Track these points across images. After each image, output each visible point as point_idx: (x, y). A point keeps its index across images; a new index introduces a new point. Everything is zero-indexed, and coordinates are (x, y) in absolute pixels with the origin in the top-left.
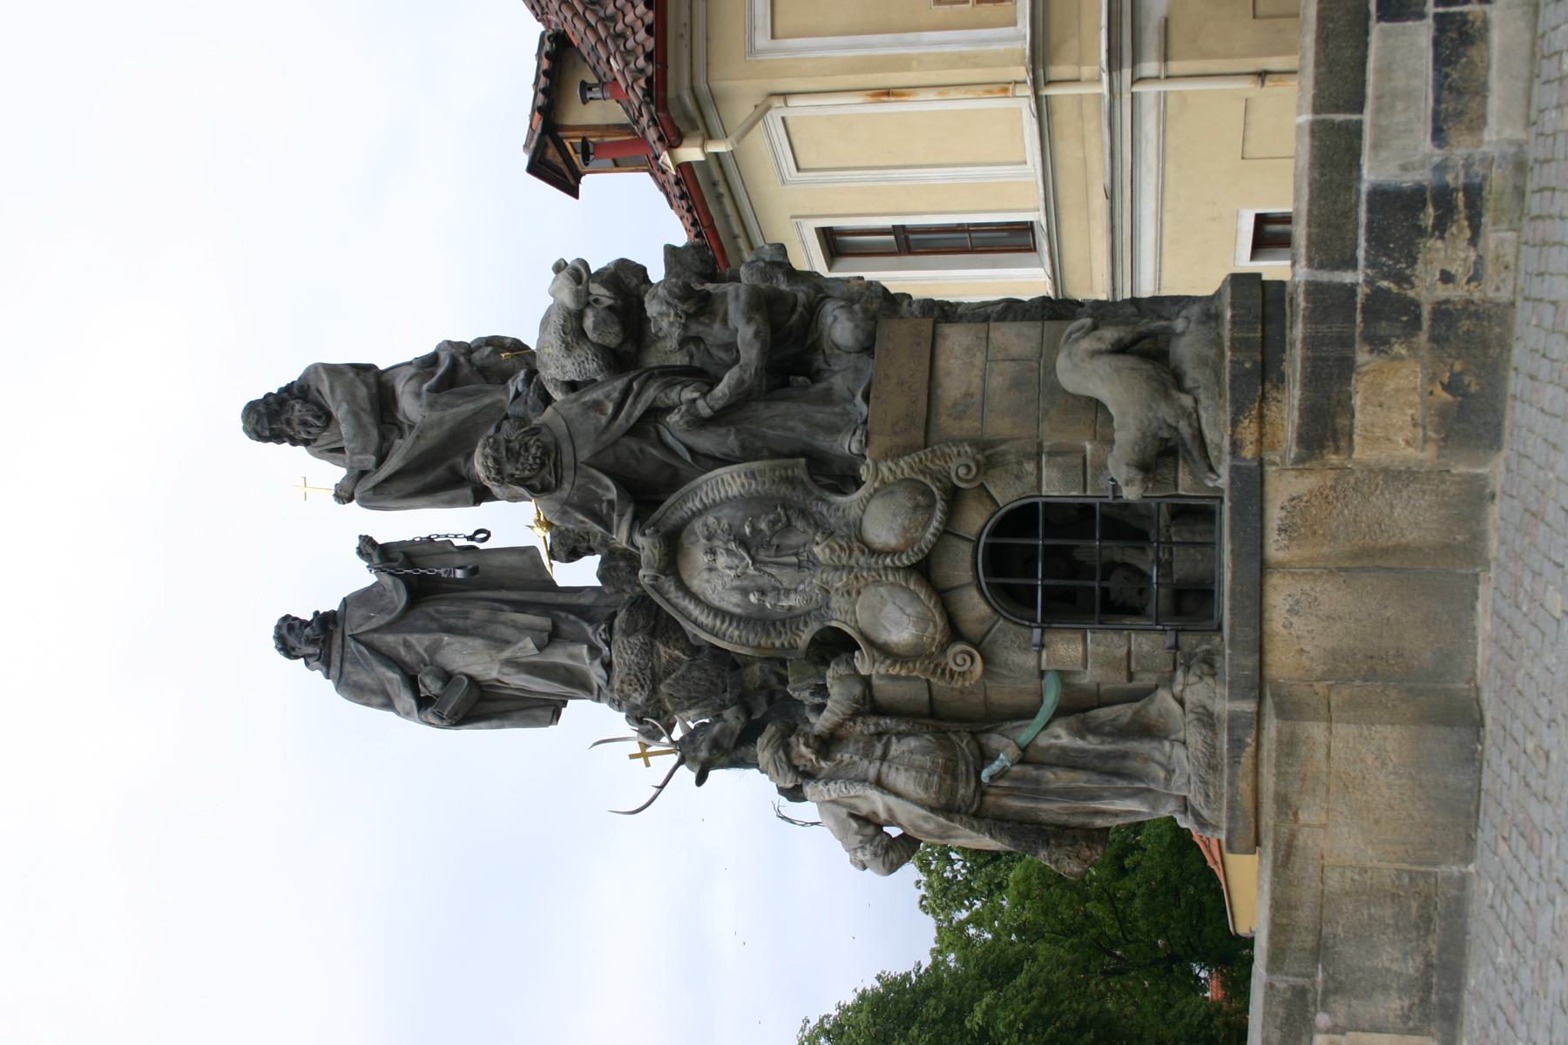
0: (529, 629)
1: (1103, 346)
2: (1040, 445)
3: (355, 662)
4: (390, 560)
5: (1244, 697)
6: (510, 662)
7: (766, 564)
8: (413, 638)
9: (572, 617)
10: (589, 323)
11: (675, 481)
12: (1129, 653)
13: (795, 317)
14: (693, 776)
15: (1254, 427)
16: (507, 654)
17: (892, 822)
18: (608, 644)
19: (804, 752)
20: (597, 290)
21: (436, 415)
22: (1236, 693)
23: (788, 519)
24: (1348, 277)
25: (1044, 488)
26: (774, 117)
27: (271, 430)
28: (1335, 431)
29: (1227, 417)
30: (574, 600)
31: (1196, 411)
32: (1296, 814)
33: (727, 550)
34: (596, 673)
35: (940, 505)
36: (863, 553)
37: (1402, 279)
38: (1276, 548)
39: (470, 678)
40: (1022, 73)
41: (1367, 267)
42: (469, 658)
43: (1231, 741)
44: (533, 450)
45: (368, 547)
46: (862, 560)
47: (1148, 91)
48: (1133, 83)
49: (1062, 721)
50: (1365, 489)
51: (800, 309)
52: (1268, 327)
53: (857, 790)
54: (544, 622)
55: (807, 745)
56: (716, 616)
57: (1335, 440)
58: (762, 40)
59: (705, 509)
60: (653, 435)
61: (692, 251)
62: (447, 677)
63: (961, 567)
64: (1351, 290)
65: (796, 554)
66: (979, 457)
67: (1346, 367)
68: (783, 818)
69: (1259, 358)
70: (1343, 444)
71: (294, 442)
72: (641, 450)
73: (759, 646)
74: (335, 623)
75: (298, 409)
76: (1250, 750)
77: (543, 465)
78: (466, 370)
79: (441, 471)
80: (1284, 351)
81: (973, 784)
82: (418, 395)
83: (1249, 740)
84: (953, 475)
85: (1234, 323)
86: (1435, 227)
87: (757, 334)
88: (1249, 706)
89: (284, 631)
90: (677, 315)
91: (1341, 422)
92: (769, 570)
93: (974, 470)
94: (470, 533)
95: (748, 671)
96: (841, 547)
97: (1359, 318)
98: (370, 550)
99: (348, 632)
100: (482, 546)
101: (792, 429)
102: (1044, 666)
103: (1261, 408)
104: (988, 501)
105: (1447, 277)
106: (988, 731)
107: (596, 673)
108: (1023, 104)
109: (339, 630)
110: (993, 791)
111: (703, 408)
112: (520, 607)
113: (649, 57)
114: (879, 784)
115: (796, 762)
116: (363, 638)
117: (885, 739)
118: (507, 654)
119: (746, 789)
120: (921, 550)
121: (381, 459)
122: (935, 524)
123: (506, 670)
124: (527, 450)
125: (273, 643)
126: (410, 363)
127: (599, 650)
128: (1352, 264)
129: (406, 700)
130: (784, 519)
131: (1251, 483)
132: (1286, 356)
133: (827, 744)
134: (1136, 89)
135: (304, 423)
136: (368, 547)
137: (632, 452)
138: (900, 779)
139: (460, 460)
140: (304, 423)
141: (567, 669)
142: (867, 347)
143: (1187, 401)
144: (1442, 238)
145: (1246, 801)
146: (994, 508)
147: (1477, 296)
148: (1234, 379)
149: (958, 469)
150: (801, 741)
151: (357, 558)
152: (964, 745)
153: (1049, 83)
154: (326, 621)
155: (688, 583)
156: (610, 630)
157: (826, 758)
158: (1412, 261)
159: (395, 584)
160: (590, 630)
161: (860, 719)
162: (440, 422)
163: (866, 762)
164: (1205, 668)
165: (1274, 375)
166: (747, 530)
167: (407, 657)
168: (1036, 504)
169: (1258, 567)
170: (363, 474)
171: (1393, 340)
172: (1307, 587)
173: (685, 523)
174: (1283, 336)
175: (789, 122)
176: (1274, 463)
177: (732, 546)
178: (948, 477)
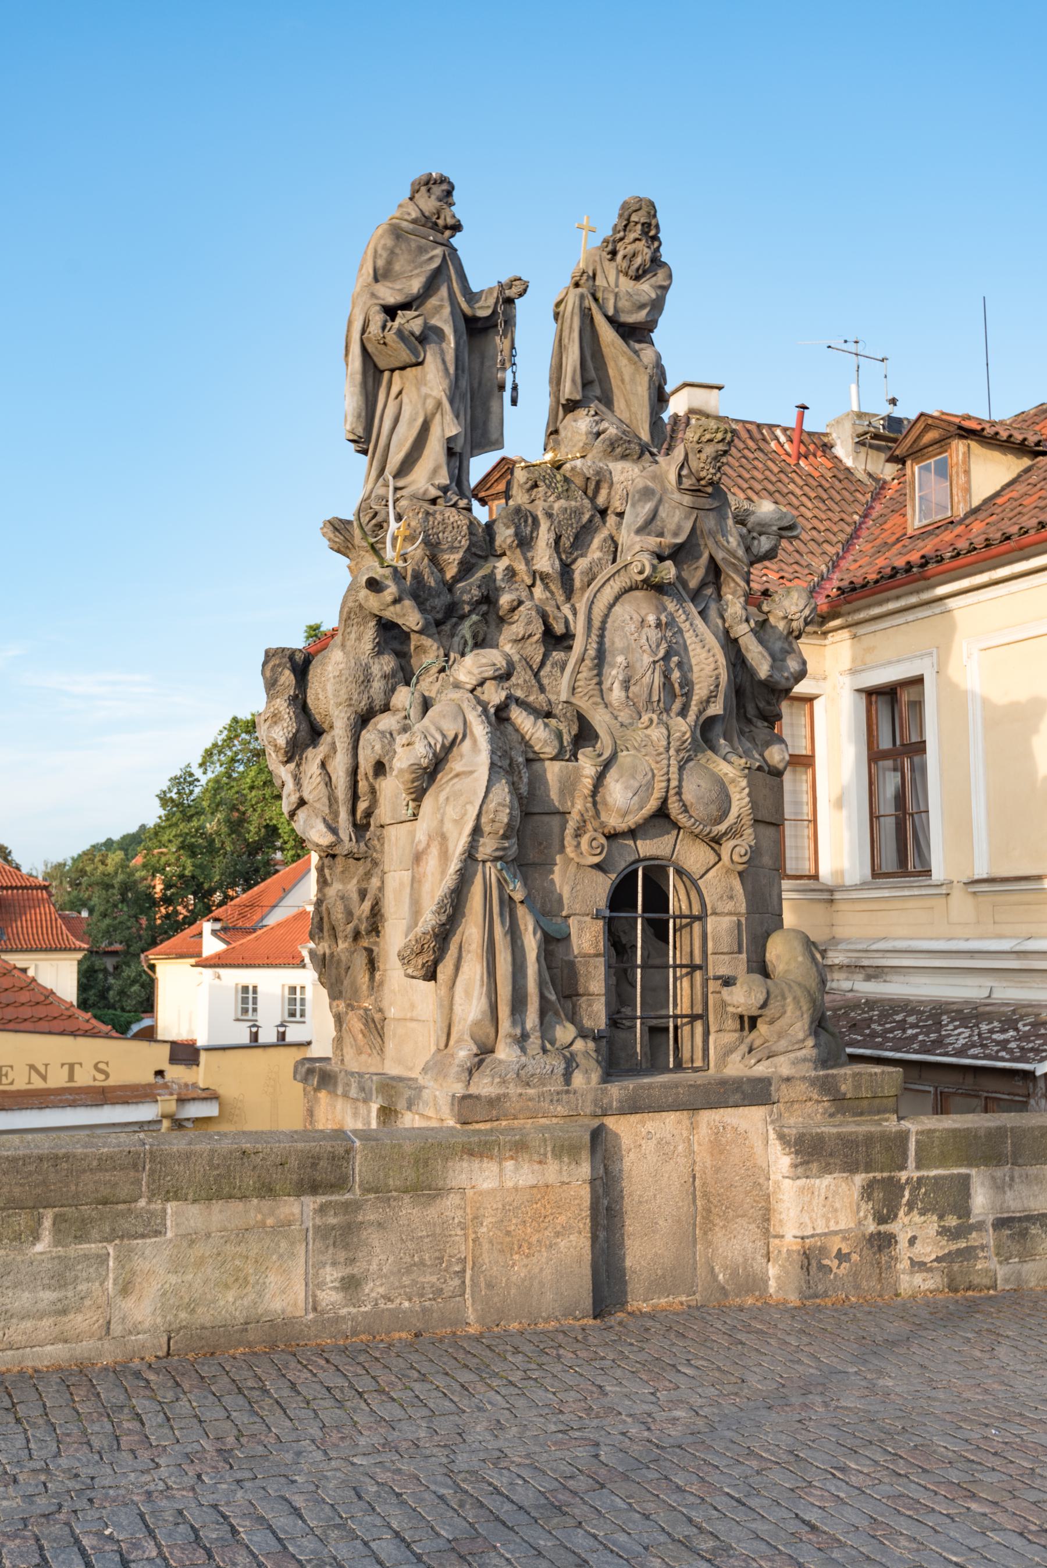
24: (911, 1162)
28: (807, 1163)
32: (512, 1158)
37: (911, 1206)
50: (754, 1193)
57: (802, 1164)
67: (851, 1168)
69: (848, 1096)
70: (800, 1170)
86: (943, 1227)
105: (912, 1241)
121: (611, 320)
128: (918, 1168)
144: (939, 1233)
147: (900, 1266)
158: (922, 1213)
171: (870, 1204)
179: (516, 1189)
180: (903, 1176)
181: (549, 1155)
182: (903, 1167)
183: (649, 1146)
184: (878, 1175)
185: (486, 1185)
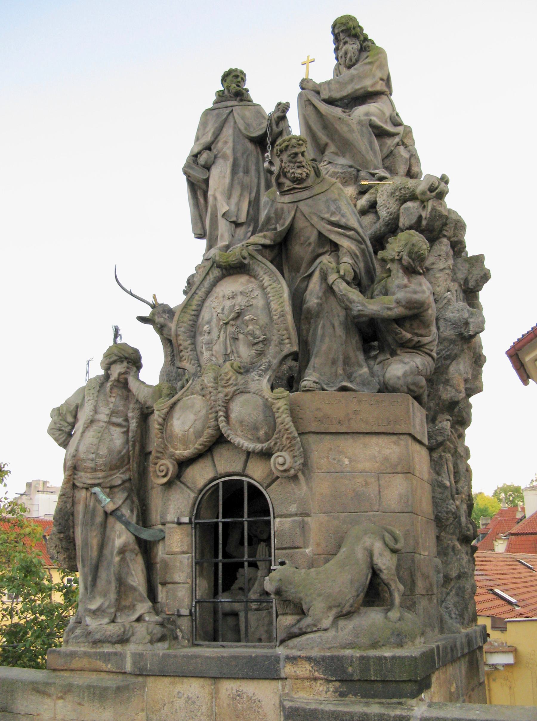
0: (239, 210)
1: (375, 558)
2: (308, 515)
3: (218, 115)
5: (134, 663)
7: (225, 332)
10: (409, 204)
12: (179, 583)
13: (409, 336)
15: (307, 674)
21: (355, 127)
22: (138, 657)
27: (339, 33)
29: (315, 653)
31: (319, 630)
32: (62, 698)
33: (234, 305)
35: (259, 446)
36: (226, 396)
38: (228, 687)
42: (219, 177)
43: (110, 654)
44: (299, 171)
45: (283, 108)
46: (221, 395)
49: (131, 539)
51: (416, 339)
52: (380, 685)
54: (243, 218)
55: (120, 374)
56: (198, 305)
59: (263, 288)
60: (321, 251)
61: (482, 274)
62: (207, 167)
63: (226, 464)
65: (232, 352)
68: (88, 364)
69: (356, 678)
71: (336, 50)
73: (177, 335)
74: (242, 100)
75: (352, 47)
76: (104, 667)
78: (390, 142)
79: (323, 138)
80: (363, 696)
81: (89, 482)
82: (367, 114)
83: (109, 666)
85: (380, 658)
88: (129, 667)
89: (235, 74)
96: (229, 379)
99: (234, 108)
101: (322, 341)
102: (168, 525)
103: (321, 679)
104: (269, 480)
111: (332, 278)
116: (231, 117)
117: (124, 423)
124: (299, 167)
125: (227, 70)
126: (394, 109)
130: (255, 341)
131: (267, 671)
132: (359, 699)
135: (346, 53)
136: (283, 108)
137: (309, 238)
139: (332, 148)
140: (346, 53)
142: (385, 388)
143: (326, 622)
145: (76, 664)
146: (265, 485)
148: (339, 659)
151: (275, 104)
152: (118, 475)
154: (241, 95)
155: (218, 284)
159: (263, 128)
162: (351, 131)
163: (108, 412)
164: (159, 636)
165: (344, 689)
166: (247, 318)
167: (220, 144)
168: (269, 515)
169: (216, 674)
170: (318, 93)
172: (204, 709)
173: (255, 277)
174: (374, 696)
176: (283, 688)
177: (237, 308)
178: (278, 451)
183: (180, 703)
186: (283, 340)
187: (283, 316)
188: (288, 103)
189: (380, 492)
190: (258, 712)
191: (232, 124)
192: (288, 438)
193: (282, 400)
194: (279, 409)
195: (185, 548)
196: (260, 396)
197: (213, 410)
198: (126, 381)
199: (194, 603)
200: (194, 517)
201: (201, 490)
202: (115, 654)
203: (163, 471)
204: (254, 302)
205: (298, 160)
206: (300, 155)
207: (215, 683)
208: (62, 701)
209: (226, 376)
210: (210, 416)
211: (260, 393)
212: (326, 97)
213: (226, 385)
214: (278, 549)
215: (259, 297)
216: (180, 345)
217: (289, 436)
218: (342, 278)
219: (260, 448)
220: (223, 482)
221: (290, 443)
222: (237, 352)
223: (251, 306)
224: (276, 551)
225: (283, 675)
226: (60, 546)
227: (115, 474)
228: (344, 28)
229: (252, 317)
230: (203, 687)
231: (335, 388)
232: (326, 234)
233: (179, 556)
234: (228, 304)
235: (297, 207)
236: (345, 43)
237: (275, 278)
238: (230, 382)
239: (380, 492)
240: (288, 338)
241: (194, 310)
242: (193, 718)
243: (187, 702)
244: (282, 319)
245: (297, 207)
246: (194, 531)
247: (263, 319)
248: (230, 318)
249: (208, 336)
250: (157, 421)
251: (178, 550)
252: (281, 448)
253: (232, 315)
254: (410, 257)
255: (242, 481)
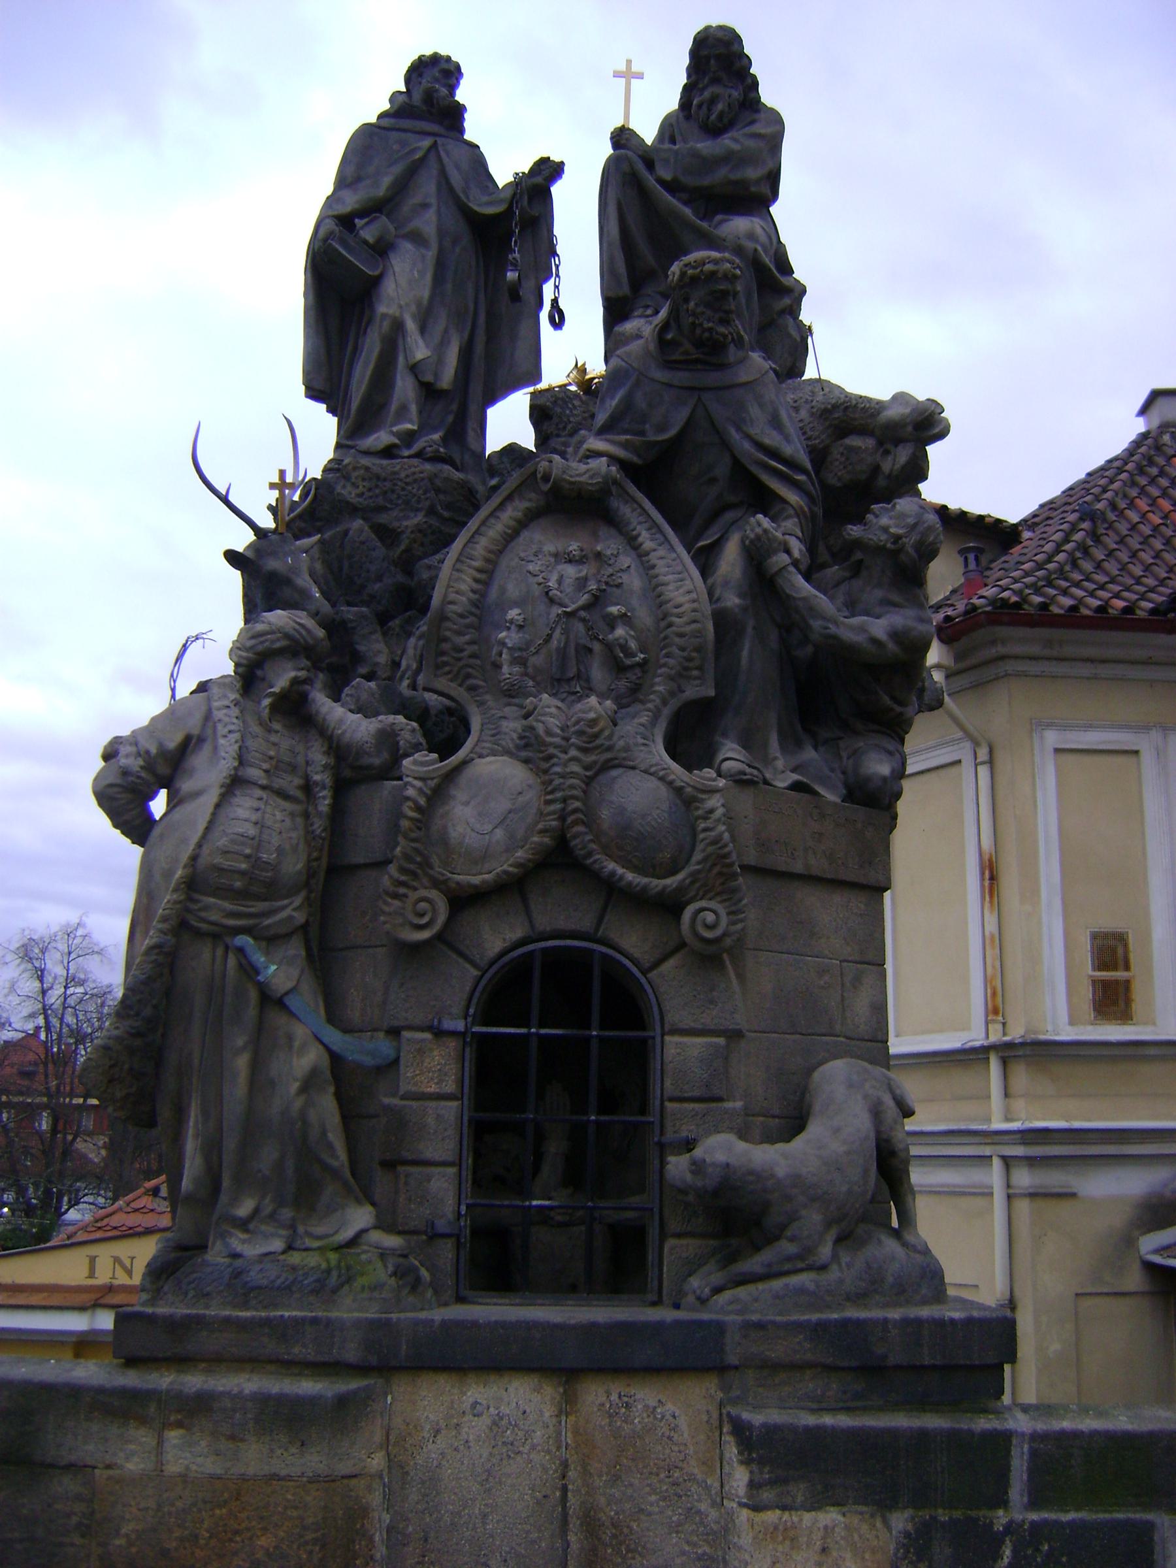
4: (530, 200)
6: (398, 326)
7: (566, 632)
8: (431, 215)
9: (450, 418)
11: (681, 519)
14: (240, 548)
16: (411, 325)
17: (173, 803)
18: (419, 455)
19: (282, 677)
20: (902, 455)
23: (632, 667)
24: (1017, 1492)
25: (677, 1039)
26: (963, 751)
27: (708, 58)
28: (785, 1481)
30: (471, 425)
34: (382, 438)
35: (657, 884)
39: (376, 281)
40: (1016, 1033)
41: (1033, 1523)
42: (404, 283)
43: (298, 1322)
44: (722, 330)
45: (547, 172)
47: (995, 1175)
48: (1004, 1158)
49: (325, 1061)
51: (898, 709)
53: (228, 747)
55: (295, 681)
57: (772, 1483)
58: (1052, 738)
59: (641, 555)
64: (1004, 1503)
65: (578, 676)
66: (728, 942)
67: (883, 1500)
68: (185, 647)
70: (767, 1495)
71: (687, 90)
72: (713, 480)
77: (699, 344)
81: (232, 922)
84: (703, 903)
87: (875, 641)
89: (445, 66)
90: (897, 538)
91: (799, 1490)
92: (557, 634)
93: (708, 935)
94: (562, 304)
95: (378, 636)
97: (957, 1514)
98: (546, 173)
99: (440, 141)
100: (544, 316)
102: (406, 1034)
106: (308, 949)
107: (382, 438)
108: (974, 1035)
109: (442, 131)
110: (220, 952)
112: (466, 354)
113: (1044, 607)
114: (235, 783)
115: (267, 666)
117: (299, 794)
118: (411, 325)
119: (219, 613)
120: (590, 854)
121: (672, 187)
122: (630, 876)
123: (386, 324)
125: (428, 52)
127: (409, 446)
128: (1034, 1503)
129: (351, 202)
130: (628, 662)
133: (294, 709)
134: (996, 1161)
135: (713, 101)
136: (547, 172)
138: (244, 810)
140: (713, 101)
141: (383, 406)
149: (706, 916)
150: (302, 674)
153: (1005, 1062)
154: (454, 115)
156: (436, 459)
157: (274, 708)
159: (501, 201)
160: (436, 437)
161: (332, 761)
166: (614, 610)
170: (650, 164)
172: (538, 1436)
175: (953, 770)
179: (184, 1477)
180: (1001, 1518)
181: (251, 1424)
182: (1004, 1503)
184: (943, 1516)
185: (133, 1466)
186: (686, 669)
187: (695, 621)
188: (562, 163)
189: (843, 999)
190: (670, 1438)
191: (435, 172)
192: (720, 874)
193: (718, 795)
194: (712, 811)
195: (450, 1087)
196: (661, 779)
197: (559, 795)
198: (303, 699)
199: (463, 1209)
200: (470, 1019)
201: (492, 964)
202: (315, 1321)
203: (422, 915)
204: (625, 578)
205: (727, 308)
206: (731, 299)
207: (567, 1382)
208: (181, 1431)
209: (591, 727)
210: (552, 808)
211: (661, 773)
212: (668, 176)
213: (590, 745)
214: (671, 1100)
215: (632, 570)
216: (445, 640)
217: (725, 870)
218: (795, 563)
219: (660, 888)
220: (545, 951)
221: (723, 884)
222: (588, 680)
223: (619, 586)
224: (667, 1104)
225: (733, 1359)
226: (126, 1066)
227: (283, 908)
228: (722, 50)
229: (623, 610)
230: (537, 1390)
231: (785, 784)
232: (755, 470)
233: (433, 1104)
234: (571, 571)
235: (699, 398)
236: (716, 81)
237: (658, 536)
238: (598, 742)
239: (843, 999)
240: (700, 668)
241: (479, 570)
242: (509, 1457)
243: (495, 1423)
244: (694, 626)
245: (699, 398)
246: (468, 1050)
247: (644, 616)
248: (580, 603)
249: (518, 632)
250: (415, 802)
251: (433, 1089)
252: (701, 893)
253: (584, 599)
254: (917, 551)
255: (592, 952)
